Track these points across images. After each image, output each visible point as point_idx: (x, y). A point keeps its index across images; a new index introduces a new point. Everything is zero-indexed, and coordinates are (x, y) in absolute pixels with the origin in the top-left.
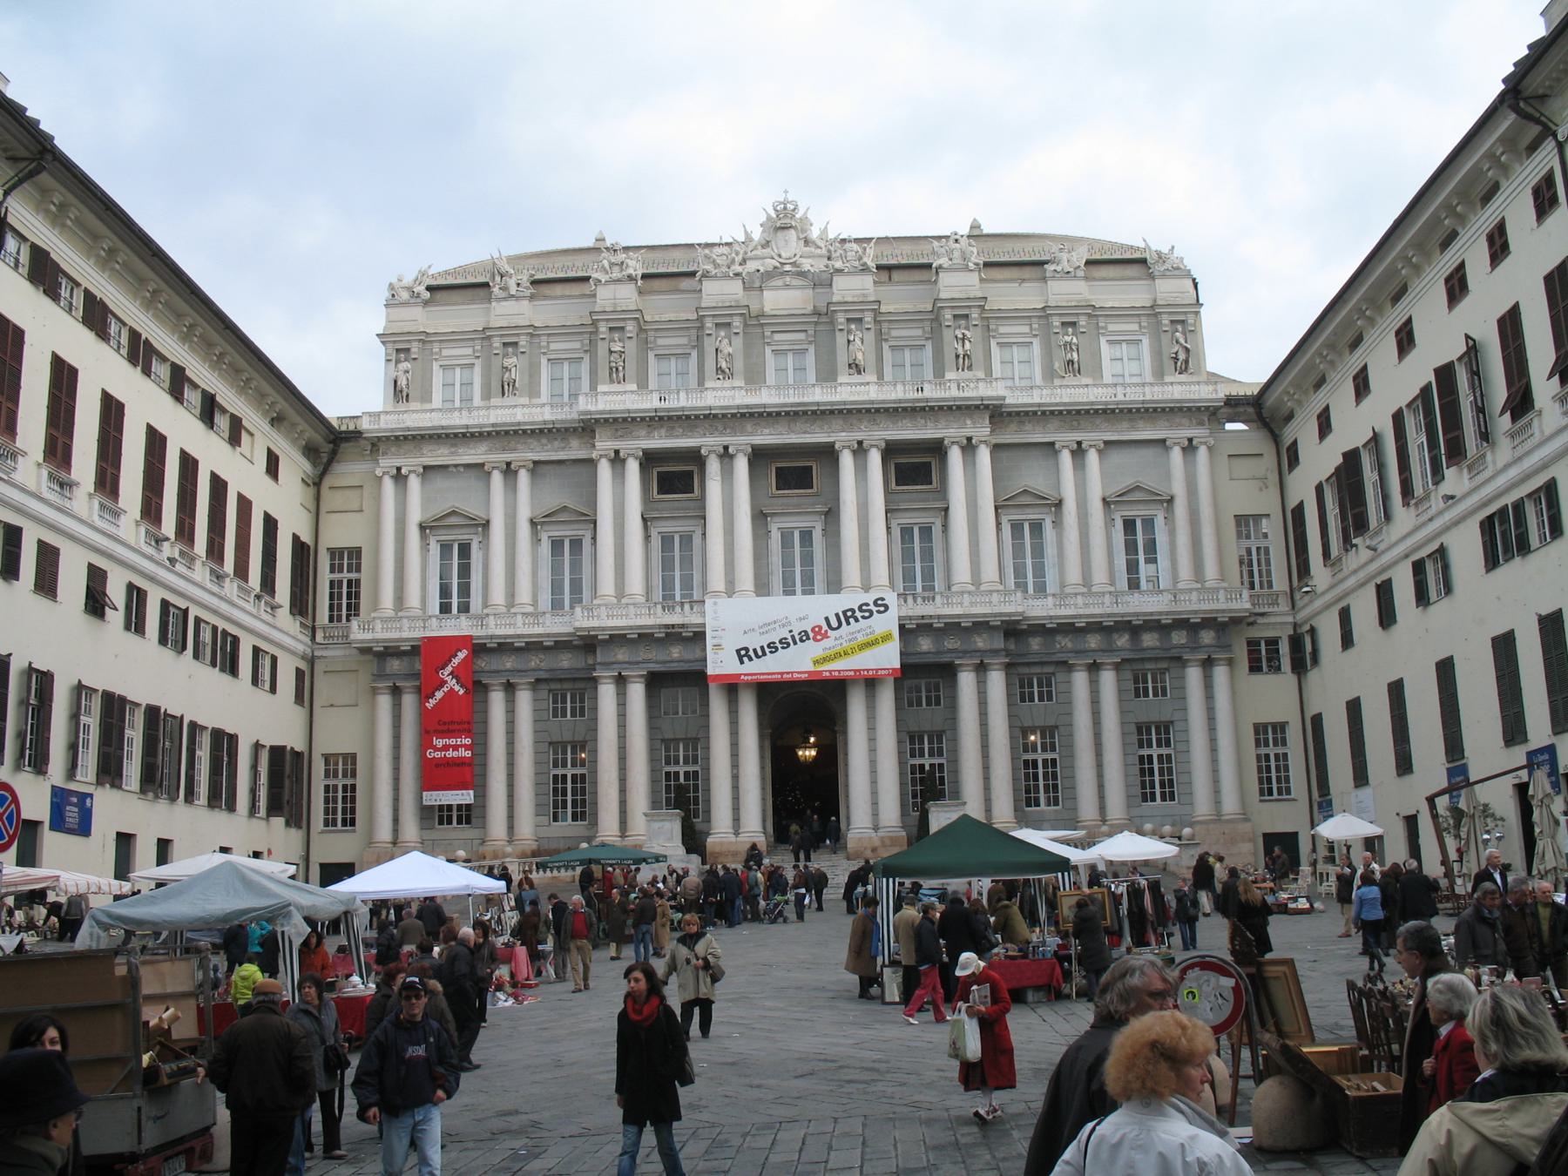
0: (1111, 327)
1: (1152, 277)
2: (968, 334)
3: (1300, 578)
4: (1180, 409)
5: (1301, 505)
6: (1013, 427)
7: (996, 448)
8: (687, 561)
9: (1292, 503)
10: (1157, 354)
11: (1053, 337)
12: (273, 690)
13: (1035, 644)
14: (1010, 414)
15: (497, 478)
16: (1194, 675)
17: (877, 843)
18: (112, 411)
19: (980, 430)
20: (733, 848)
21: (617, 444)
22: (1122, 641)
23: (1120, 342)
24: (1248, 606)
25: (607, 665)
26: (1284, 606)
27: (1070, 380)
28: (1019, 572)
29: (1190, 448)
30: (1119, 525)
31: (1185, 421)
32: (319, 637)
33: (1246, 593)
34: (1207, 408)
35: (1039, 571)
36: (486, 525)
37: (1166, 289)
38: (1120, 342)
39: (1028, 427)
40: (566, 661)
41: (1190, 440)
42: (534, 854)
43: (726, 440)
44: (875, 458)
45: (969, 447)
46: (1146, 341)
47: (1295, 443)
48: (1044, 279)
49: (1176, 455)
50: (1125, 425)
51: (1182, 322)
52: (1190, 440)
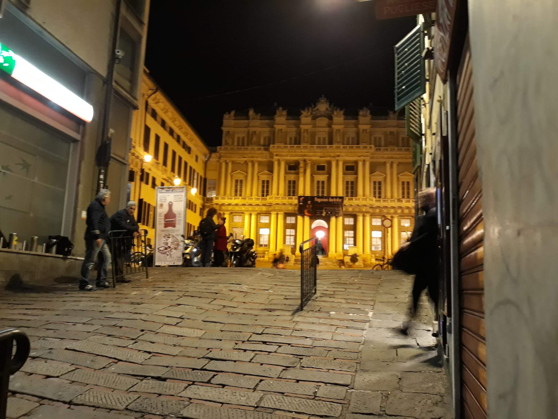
8: (294, 187)
12: (195, 212)
13: (377, 211)
15: (250, 165)
18: (166, 146)
22: (399, 211)
25: (274, 210)
28: (375, 193)
30: (401, 183)
32: (205, 200)
35: (380, 193)
36: (246, 176)
40: (264, 209)
43: (306, 158)
44: (341, 164)
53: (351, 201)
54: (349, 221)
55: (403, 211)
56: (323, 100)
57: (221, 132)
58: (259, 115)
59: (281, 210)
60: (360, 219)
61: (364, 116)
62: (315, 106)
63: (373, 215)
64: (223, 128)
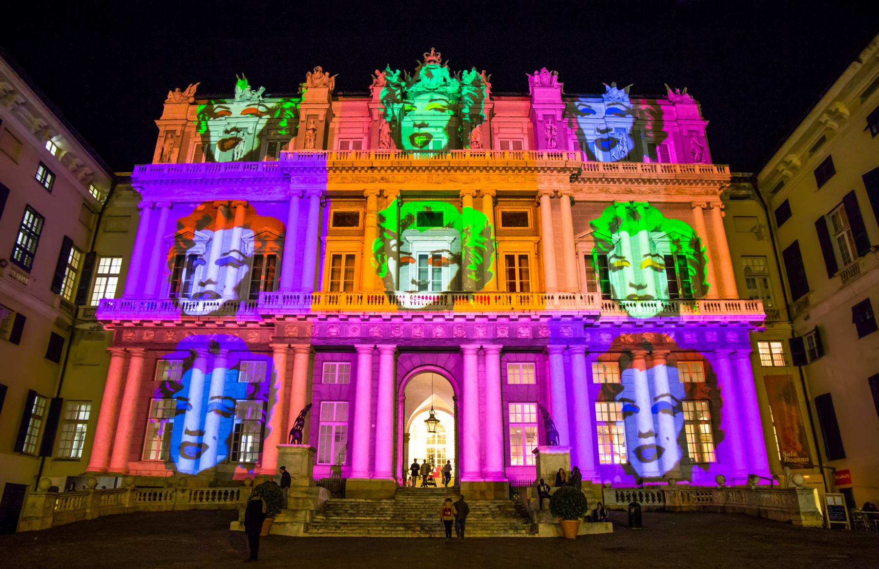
1: (674, 104)
2: (554, 127)
3: (795, 299)
5: (795, 246)
7: (573, 202)
8: (349, 272)
9: (785, 243)
12: (16, 338)
16: (724, 365)
17: (484, 488)
20: (368, 488)
21: (303, 186)
24: (763, 314)
25: (280, 339)
26: (784, 316)
29: (707, 209)
33: (760, 305)
42: (211, 485)
43: (383, 186)
44: (488, 201)
45: (556, 196)
47: (786, 203)
49: (698, 212)
52: (708, 203)
53: (525, 306)
54: (523, 374)
55: (679, 337)
56: (433, 55)
57: (156, 130)
58: (262, 89)
59: (301, 339)
60: (556, 361)
61: (543, 85)
62: (412, 76)
63: (593, 354)
64: (157, 122)
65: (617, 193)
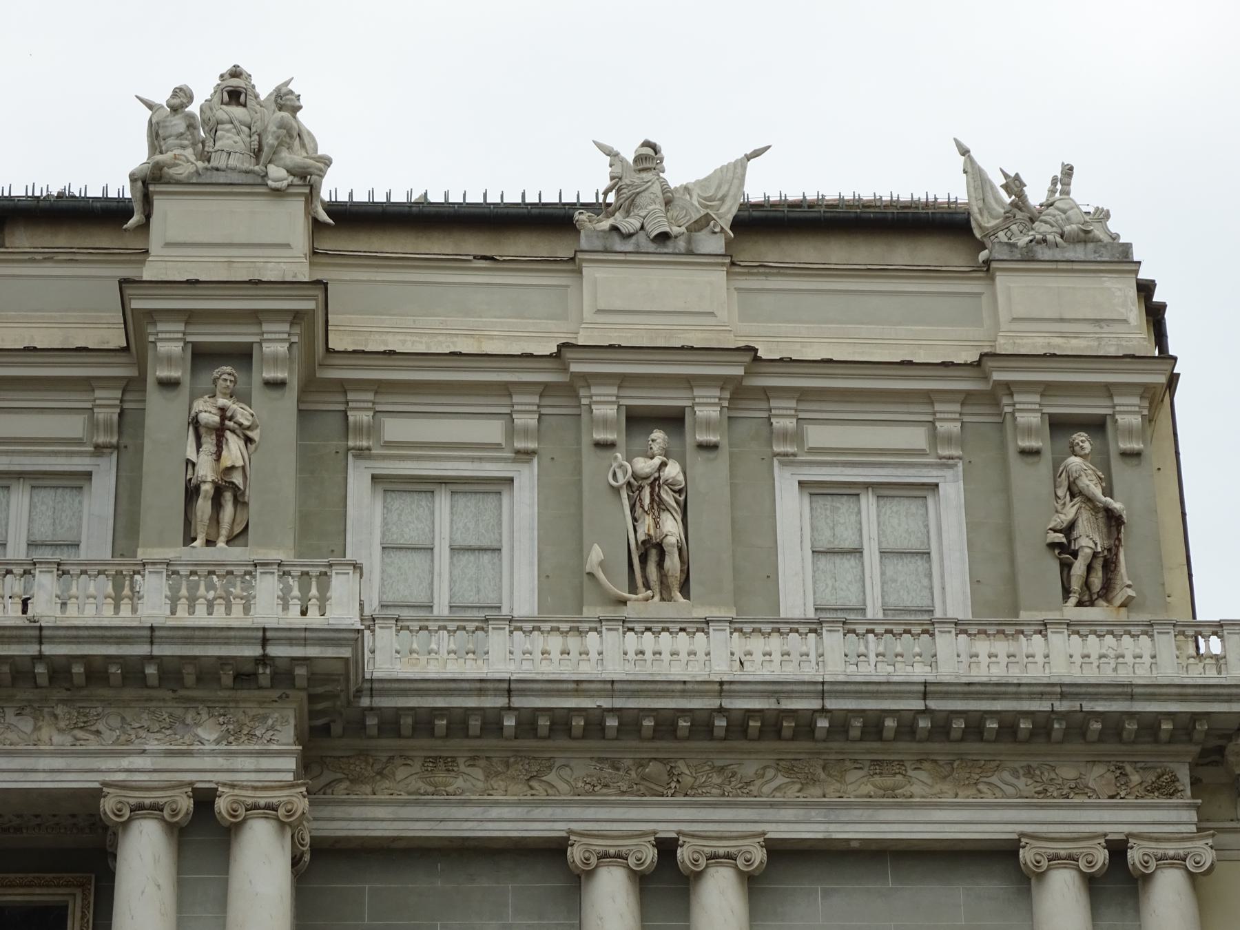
0: (817, 436)
2: (242, 414)
4: (1077, 727)
6: (407, 777)
10: (994, 533)
11: (590, 459)
14: (391, 724)
19: (255, 762)
23: (851, 491)
27: (642, 606)
31: (1097, 776)
34: (1186, 725)
37: (1029, 312)
38: (851, 491)
39: (469, 779)
41: (1118, 850)
46: (952, 490)
48: (572, 264)
50: (858, 784)
51: (1096, 426)
65: (591, 792)
